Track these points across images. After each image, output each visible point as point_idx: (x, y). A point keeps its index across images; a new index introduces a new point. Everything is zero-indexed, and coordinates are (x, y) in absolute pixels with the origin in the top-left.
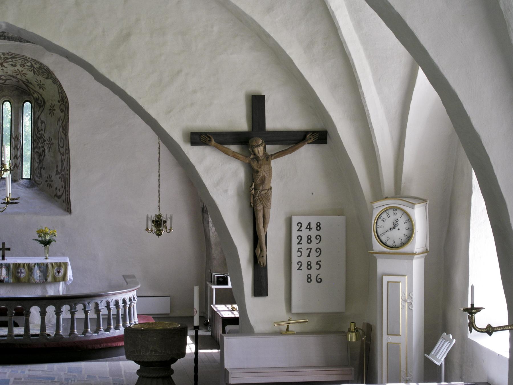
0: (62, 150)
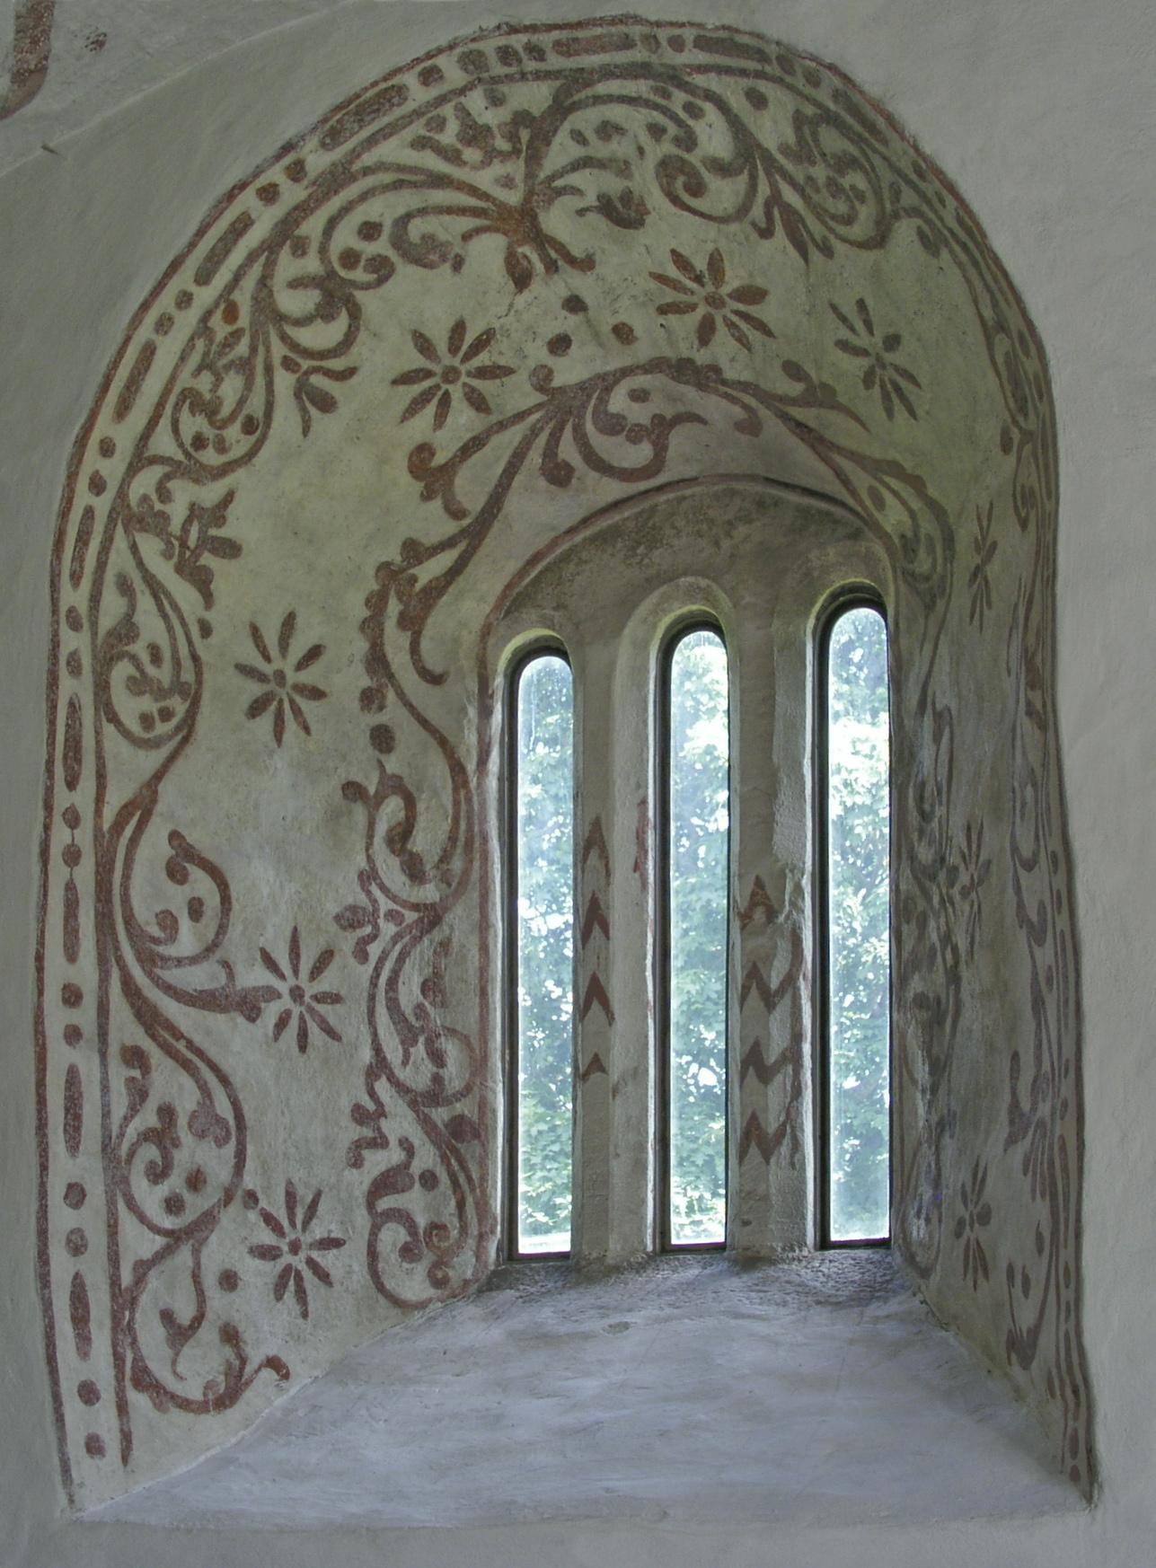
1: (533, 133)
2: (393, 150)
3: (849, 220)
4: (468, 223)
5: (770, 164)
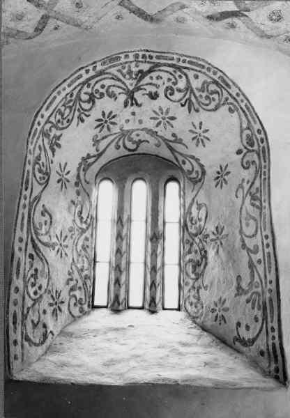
1: (142, 74)
2: (114, 71)
3: (207, 105)
4: (121, 91)
5: (192, 91)
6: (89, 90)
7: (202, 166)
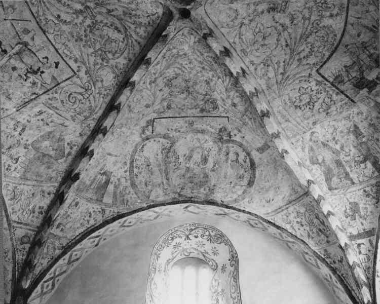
0: (233, 295)
1: (192, 230)
2: (182, 230)
5: (211, 236)
6: (172, 236)
7: (216, 264)
